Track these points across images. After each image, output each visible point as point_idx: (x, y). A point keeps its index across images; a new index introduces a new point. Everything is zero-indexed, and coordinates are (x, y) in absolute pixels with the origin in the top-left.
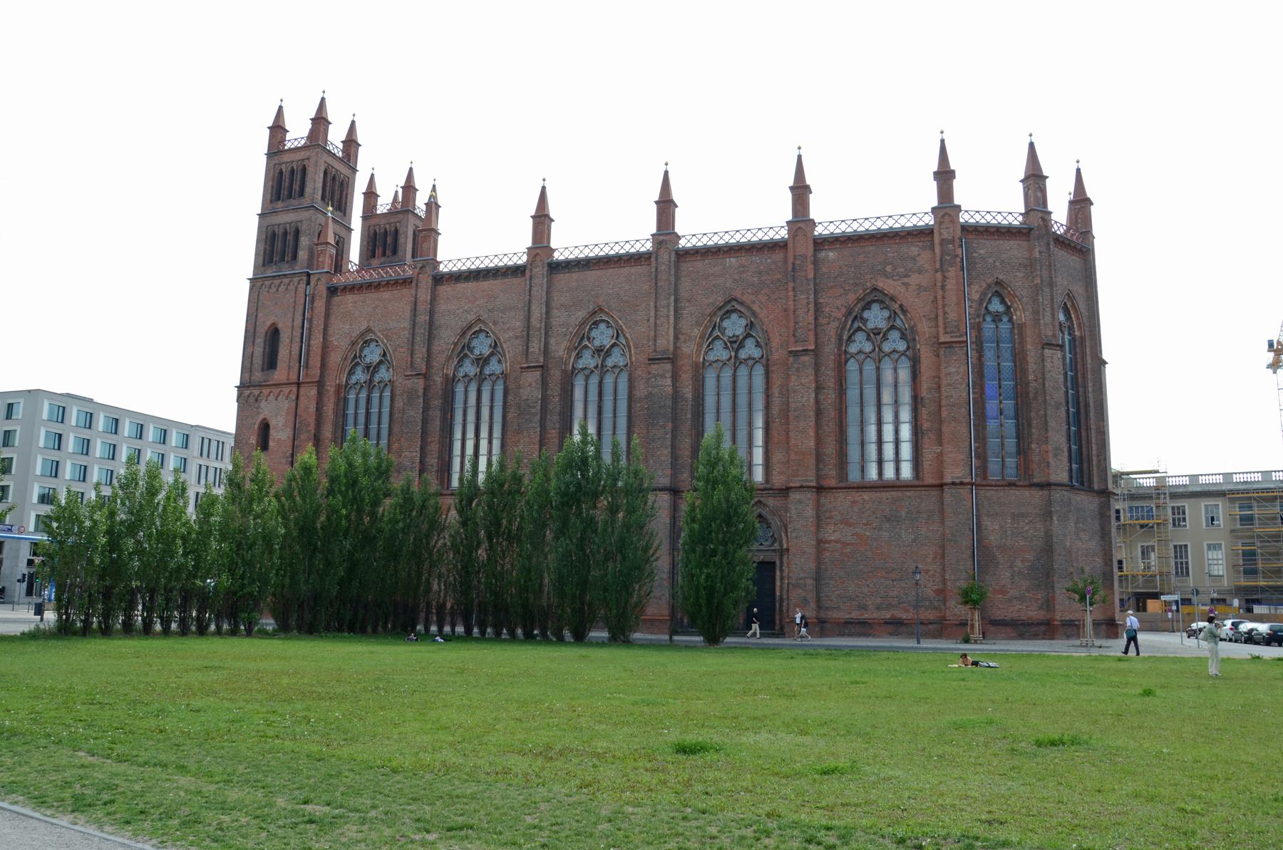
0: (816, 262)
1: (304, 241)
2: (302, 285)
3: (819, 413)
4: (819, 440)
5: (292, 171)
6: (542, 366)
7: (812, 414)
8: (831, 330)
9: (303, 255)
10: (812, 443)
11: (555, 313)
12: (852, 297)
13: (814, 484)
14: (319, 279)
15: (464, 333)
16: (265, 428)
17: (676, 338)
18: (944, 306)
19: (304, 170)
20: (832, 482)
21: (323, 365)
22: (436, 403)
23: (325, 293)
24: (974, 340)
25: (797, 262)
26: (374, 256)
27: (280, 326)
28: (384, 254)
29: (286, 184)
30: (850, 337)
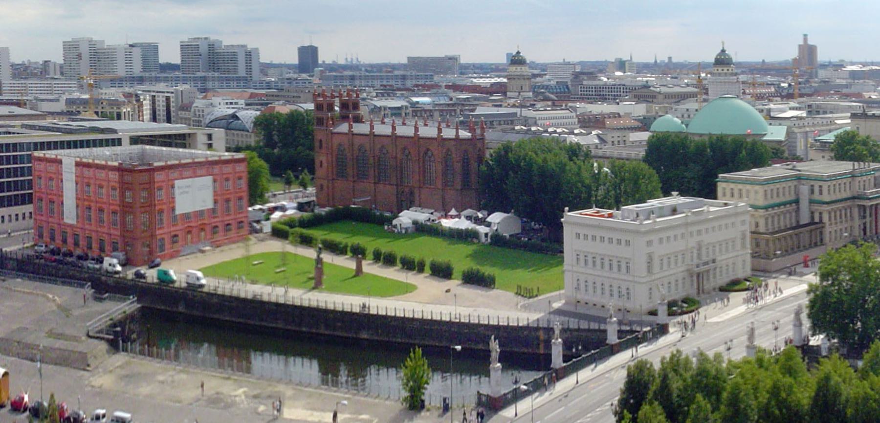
1: (325, 121)
9: (325, 124)
16: (321, 162)
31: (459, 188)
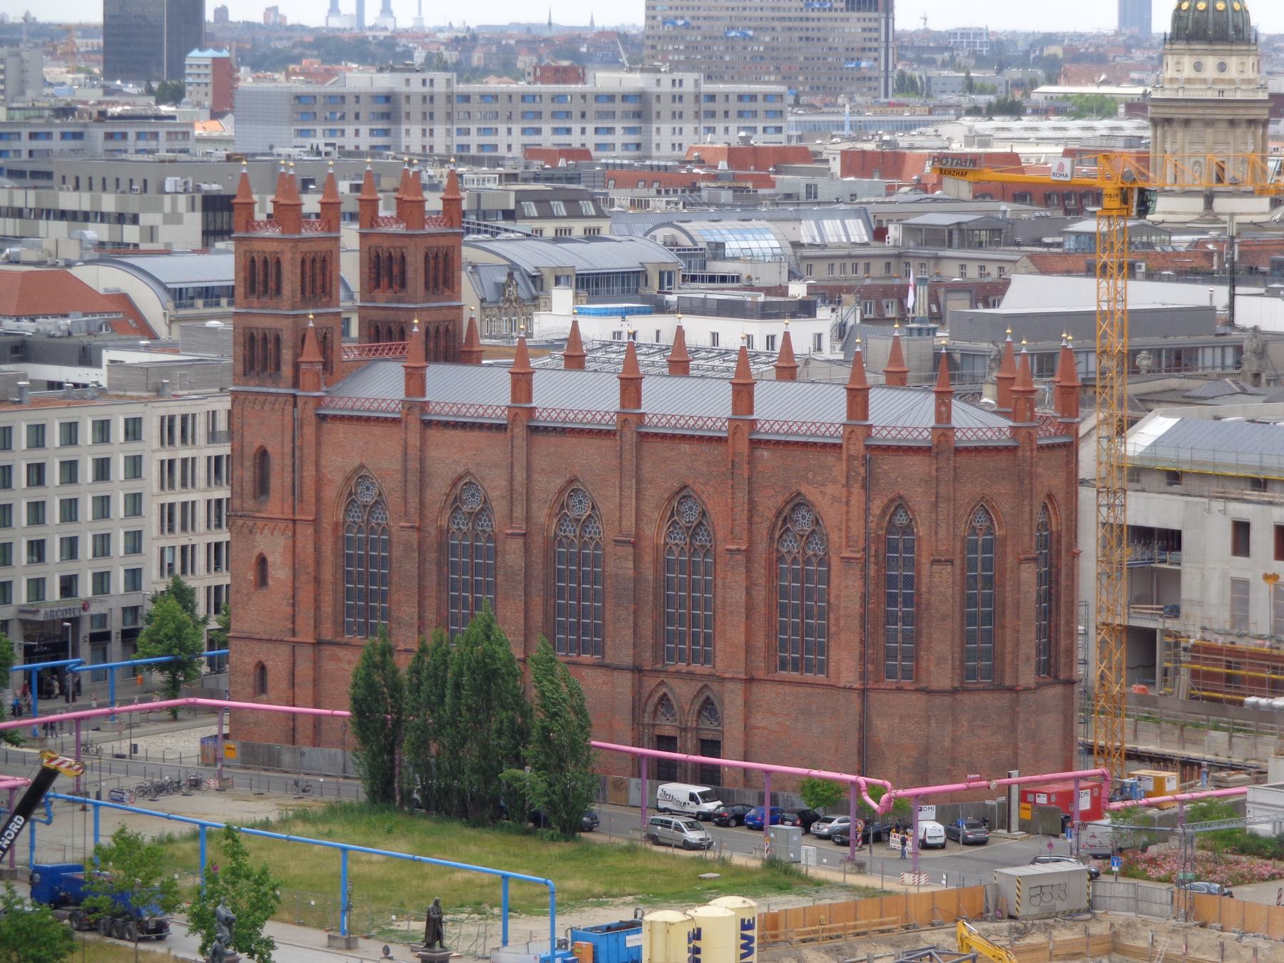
0: (752, 461)
1: (287, 355)
2: (289, 407)
3: (750, 610)
4: (749, 633)
5: (265, 262)
6: (524, 535)
7: (743, 610)
8: (763, 529)
9: (287, 370)
10: (742, 638)
11: (536, 476)
12: (780, 500)
13: (743, 676)
14: (306, 403)
15: (454, 484)
16: (262, 561)
17: (638, 519)
18: (847, 520)
19: (278, 262)
20: (760, 674)
21: (318, 499)
22: (432, 556)
23: (314, 419)
24: (873, 553)
25: (737, 460)
26: (378, 286)
27: (269, 449)
28: (390, 286)
29: (260, 277)
30: (781, 536)
31: (942, 678)
